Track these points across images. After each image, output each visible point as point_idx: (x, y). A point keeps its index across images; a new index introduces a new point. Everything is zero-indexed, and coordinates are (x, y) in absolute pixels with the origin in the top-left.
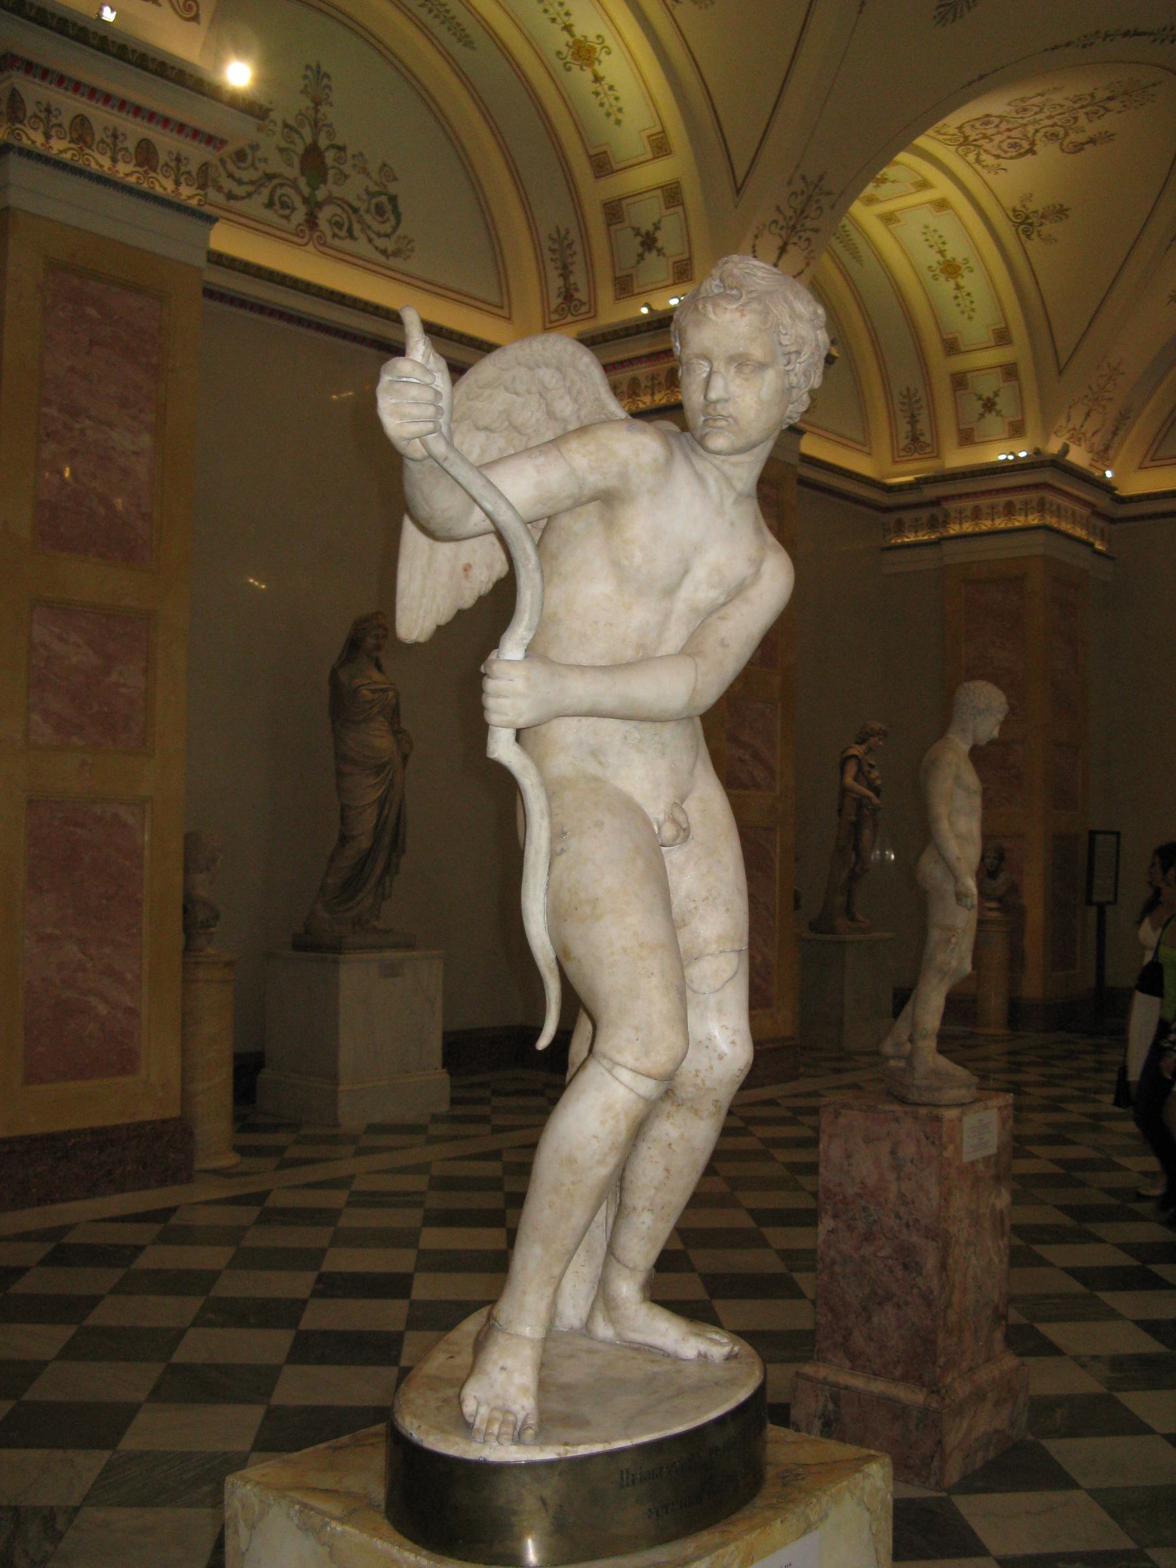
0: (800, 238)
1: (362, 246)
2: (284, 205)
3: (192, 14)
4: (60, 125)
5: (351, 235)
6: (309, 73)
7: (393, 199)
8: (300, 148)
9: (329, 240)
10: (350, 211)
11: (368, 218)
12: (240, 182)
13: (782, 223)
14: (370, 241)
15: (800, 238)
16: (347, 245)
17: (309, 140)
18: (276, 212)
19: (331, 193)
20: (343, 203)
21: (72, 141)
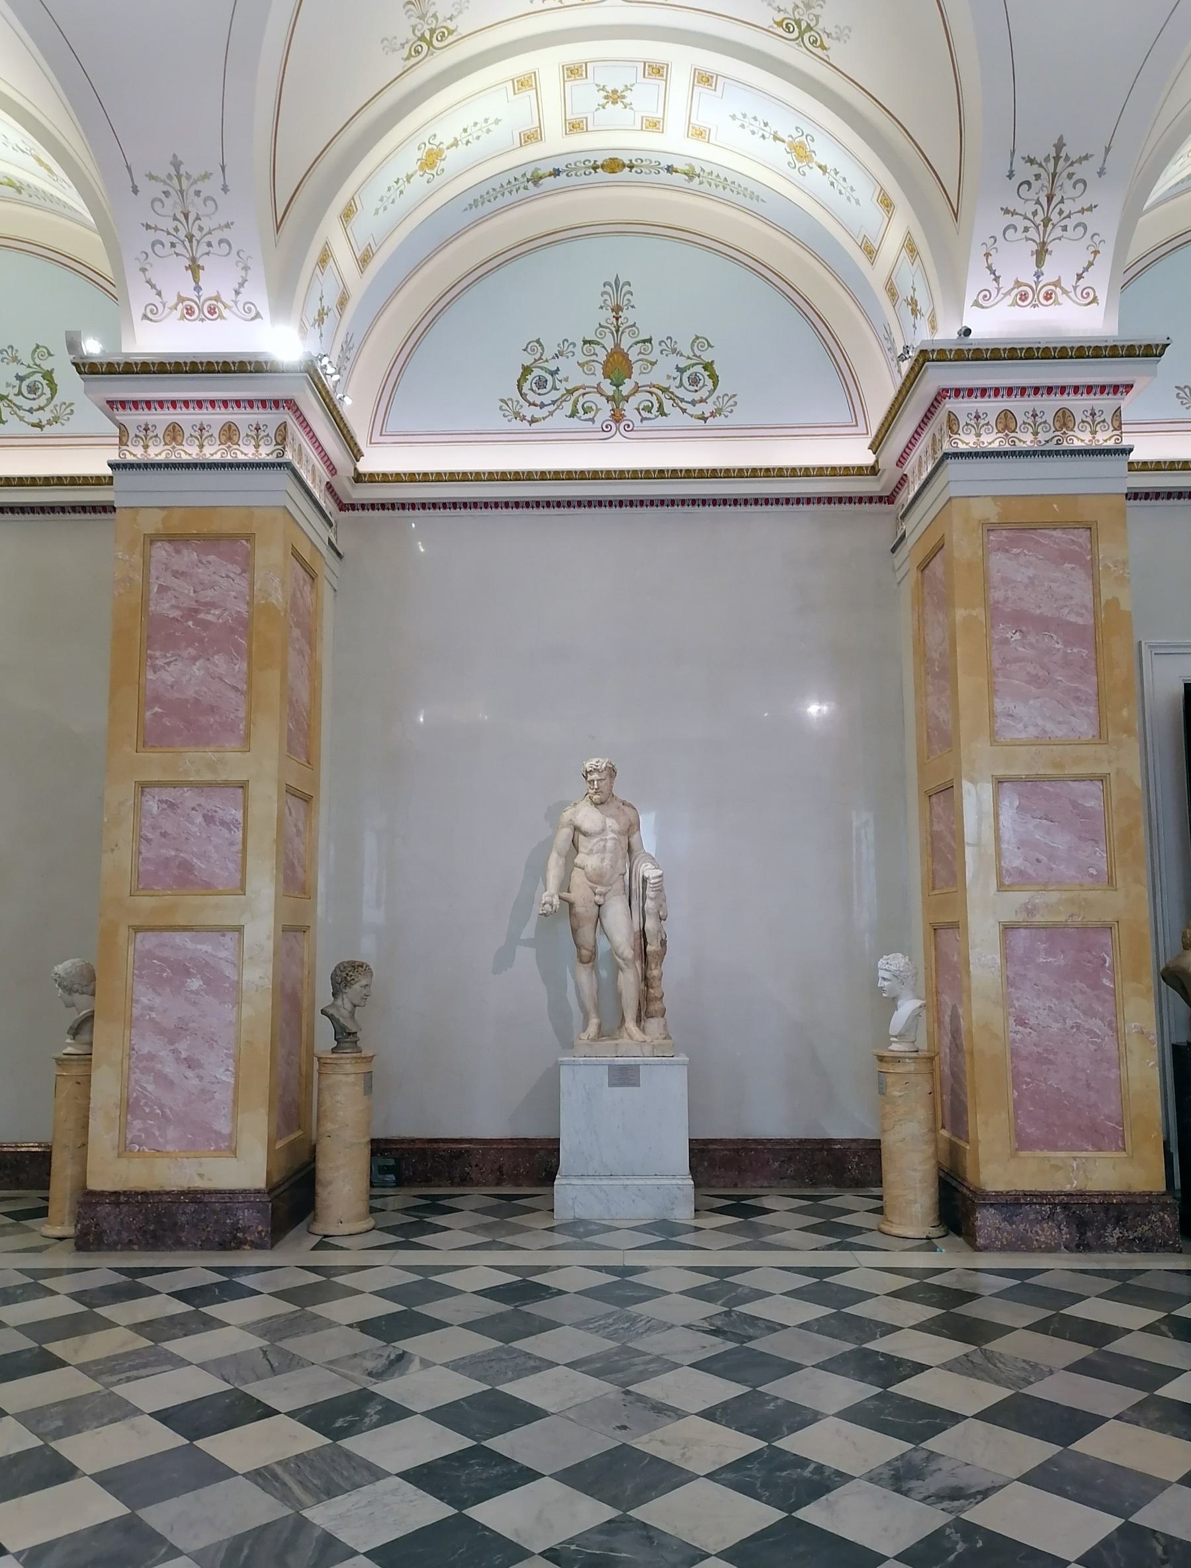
0: (1065, 228)
1: (675, 416)
3: (253, 314)
5: (663, 414)
6: (608, 289)
7: (708, 367)
8: (602, 357)
9: (637, 422)
11: (680, 393)
12: (542, 406)
13: (1020, 223)
14: (684, 411)
15: (1065, 228)
17: (610, 345)
18: (579, 418)
20: (651, 388)
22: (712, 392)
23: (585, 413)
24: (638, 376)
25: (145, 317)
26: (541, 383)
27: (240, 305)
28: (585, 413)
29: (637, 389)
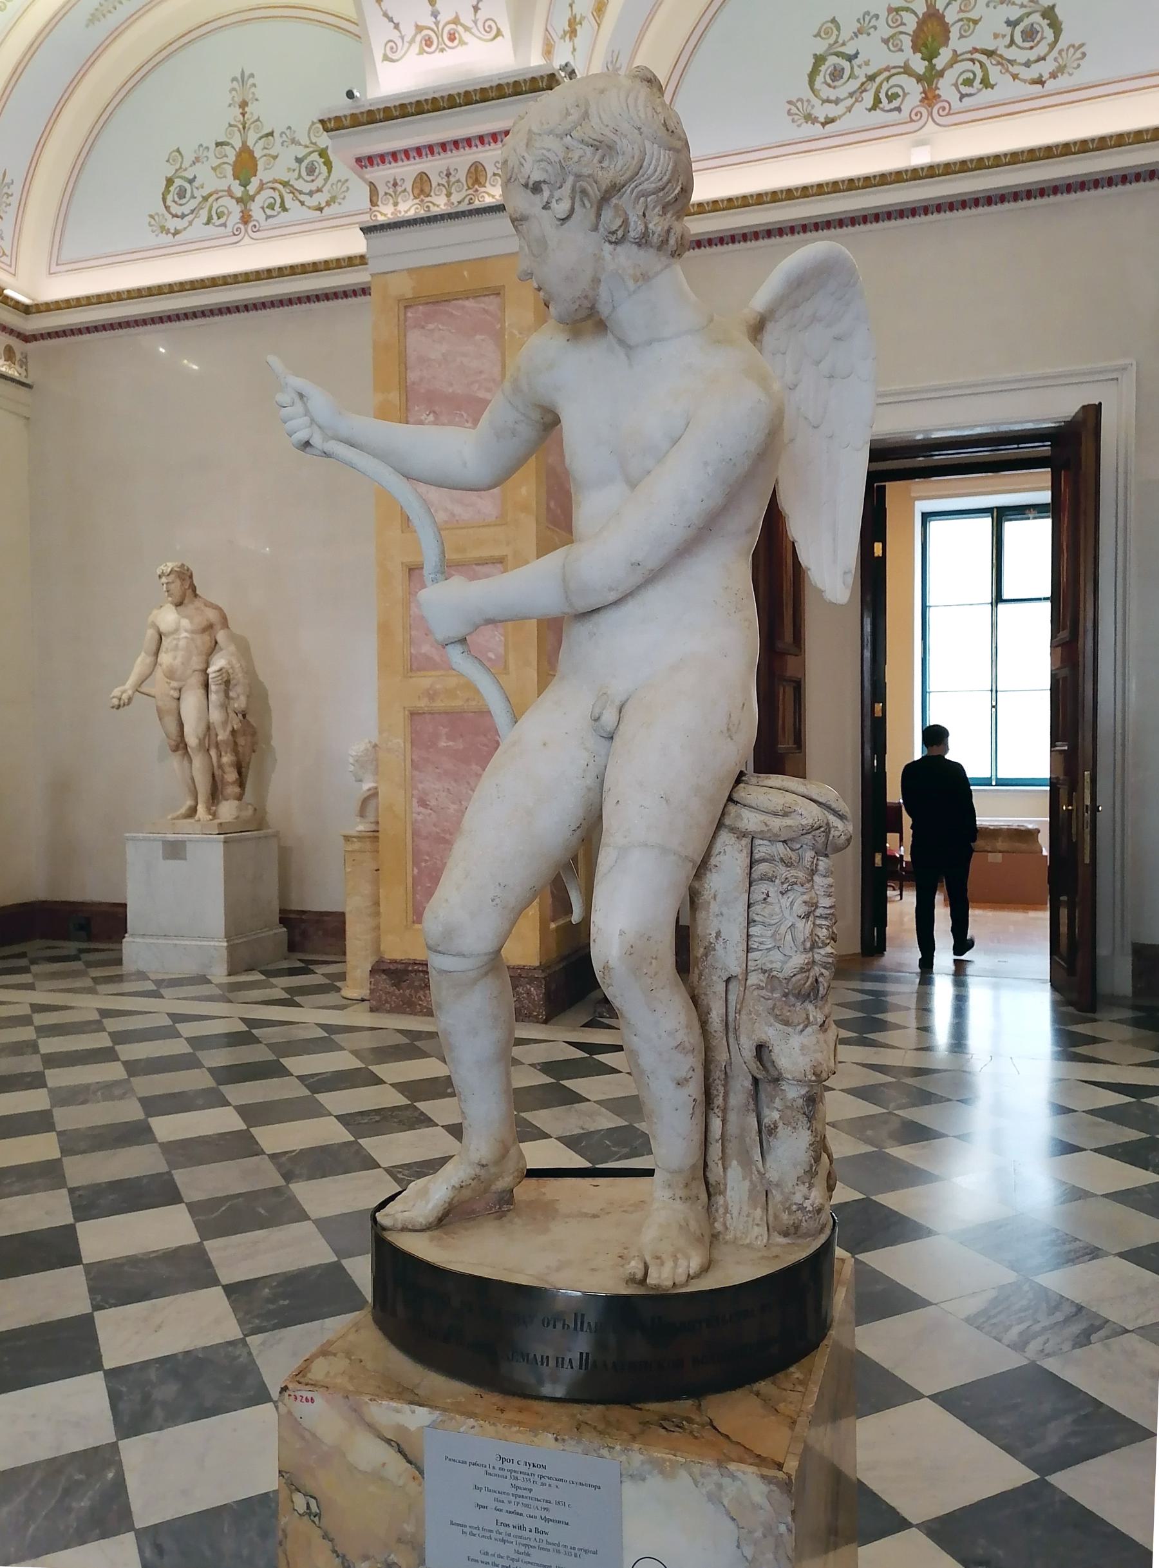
2: (891, 98)
3: (494, 32)
4: (458, 181)
5: (986, 83)
9: (956, 105)
10: (983, 58)
11: (1012, 53)
14: (1015, 77)
16: (987, 95)
19: (955, 51)
21: (415, 198)
22: (1052, 46)
23: (890, 101)
24: (956, 43)
25: (386, 58)
26: (836, 74)
27: (480, 24)
28: (890, 101)
29: (955, 59)
